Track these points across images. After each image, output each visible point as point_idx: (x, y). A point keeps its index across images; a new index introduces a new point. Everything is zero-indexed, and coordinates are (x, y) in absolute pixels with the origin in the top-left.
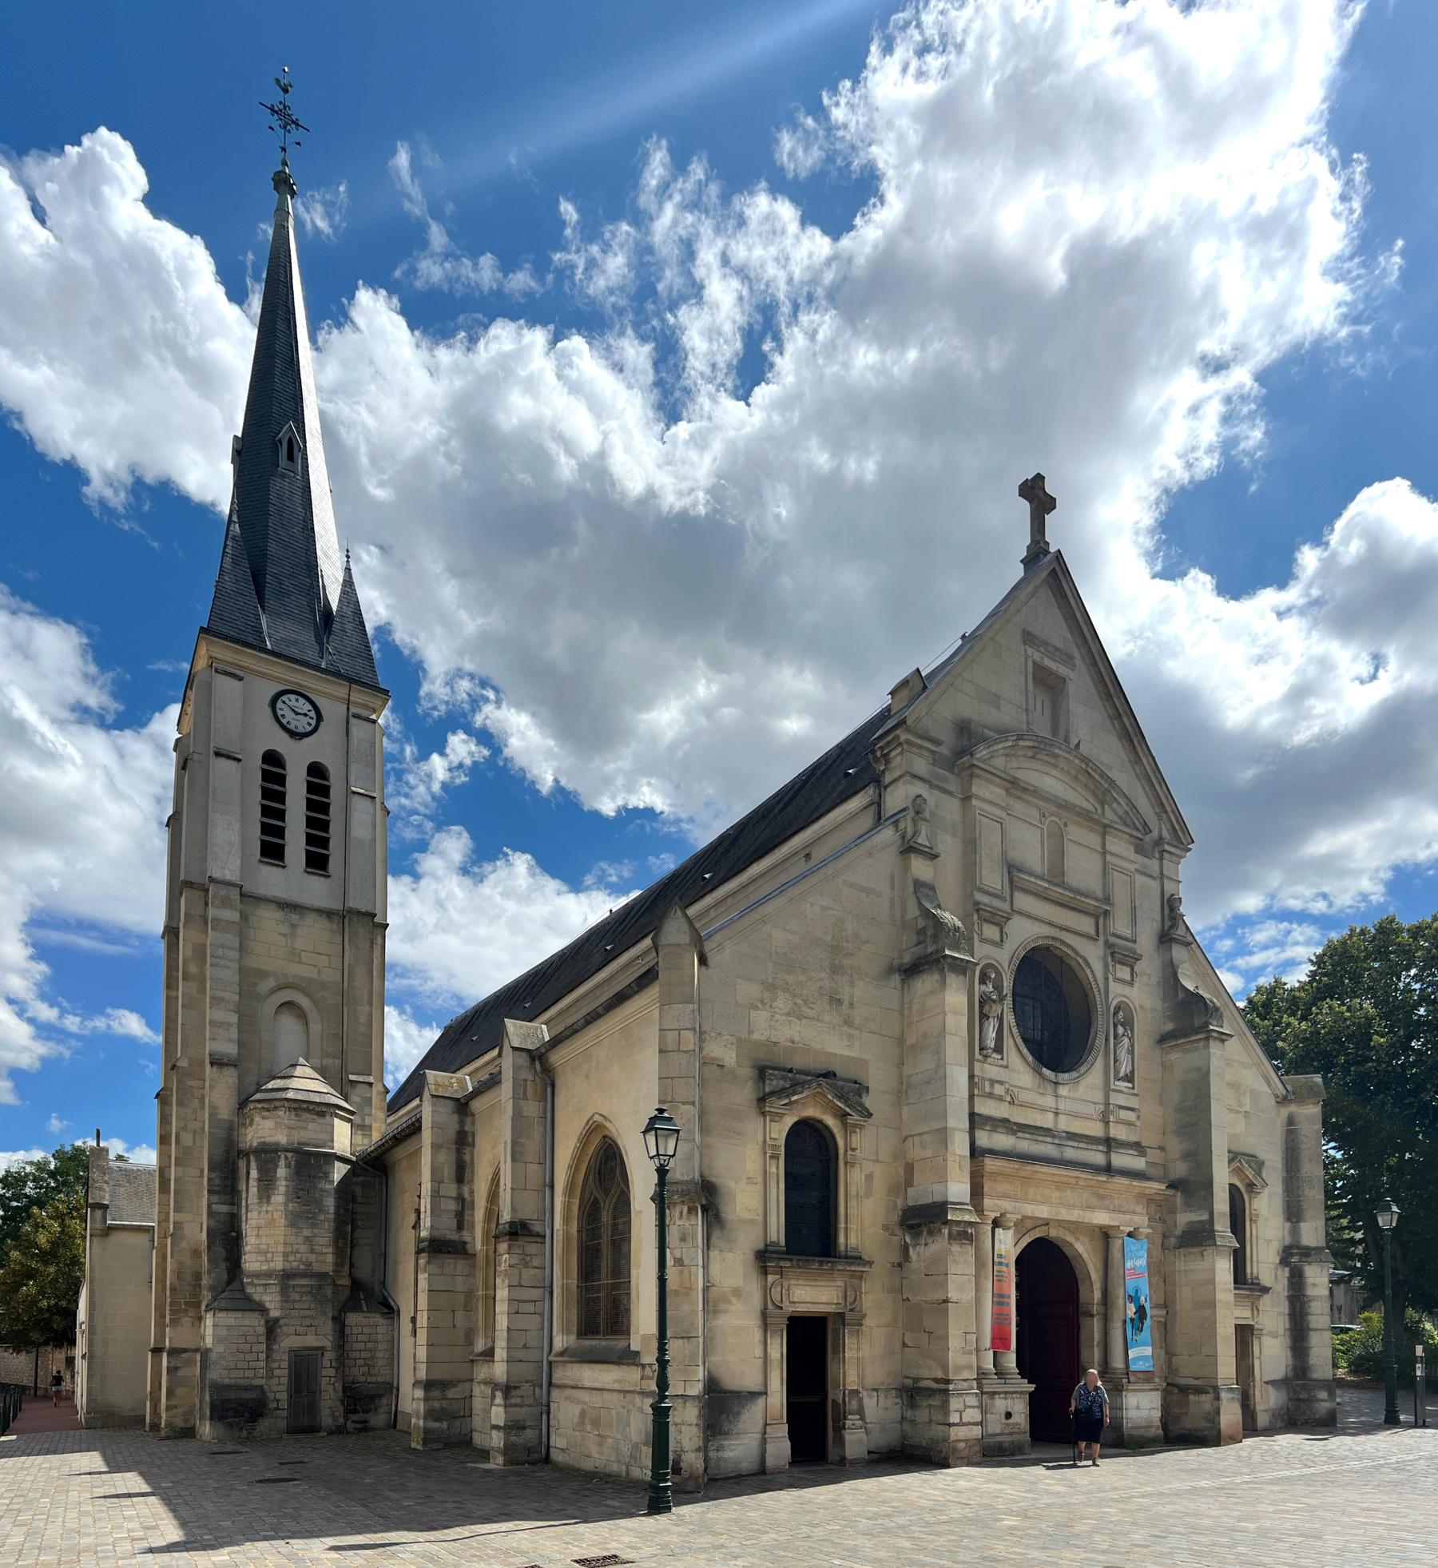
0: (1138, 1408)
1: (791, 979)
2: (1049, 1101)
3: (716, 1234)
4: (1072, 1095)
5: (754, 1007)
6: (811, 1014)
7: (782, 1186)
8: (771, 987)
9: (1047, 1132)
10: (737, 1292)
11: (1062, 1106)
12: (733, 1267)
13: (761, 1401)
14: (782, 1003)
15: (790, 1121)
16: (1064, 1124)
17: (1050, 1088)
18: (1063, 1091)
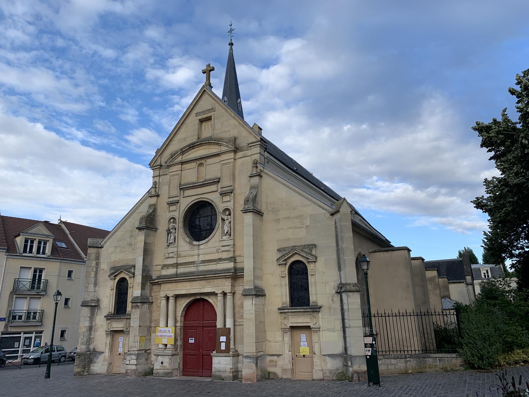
0: (219, 363)
1: (120, 243)
2: (196, 252)
3: (99, 311)
4: (206, 247)
5: (112, 253)
6: (124, 250)
7: (114, 297)
8: (116, 247)
9: (193, 263)
10: (101, 326)
11: (200, 252)
12: (100, 320)
13: (103, 355)
14: (118, 250)
15: (117, 279)
16: (202, 258)
17: (196, 247)
18: (201, 247)
